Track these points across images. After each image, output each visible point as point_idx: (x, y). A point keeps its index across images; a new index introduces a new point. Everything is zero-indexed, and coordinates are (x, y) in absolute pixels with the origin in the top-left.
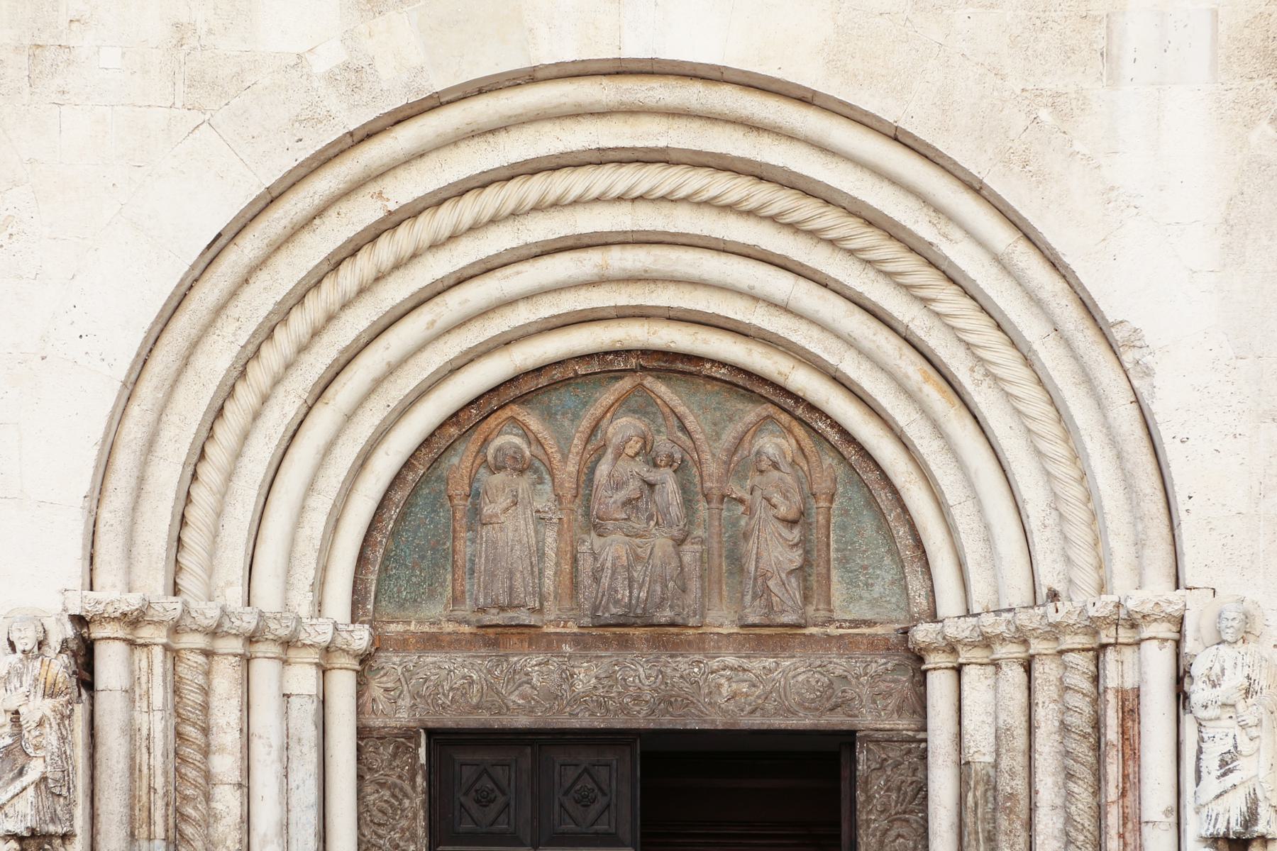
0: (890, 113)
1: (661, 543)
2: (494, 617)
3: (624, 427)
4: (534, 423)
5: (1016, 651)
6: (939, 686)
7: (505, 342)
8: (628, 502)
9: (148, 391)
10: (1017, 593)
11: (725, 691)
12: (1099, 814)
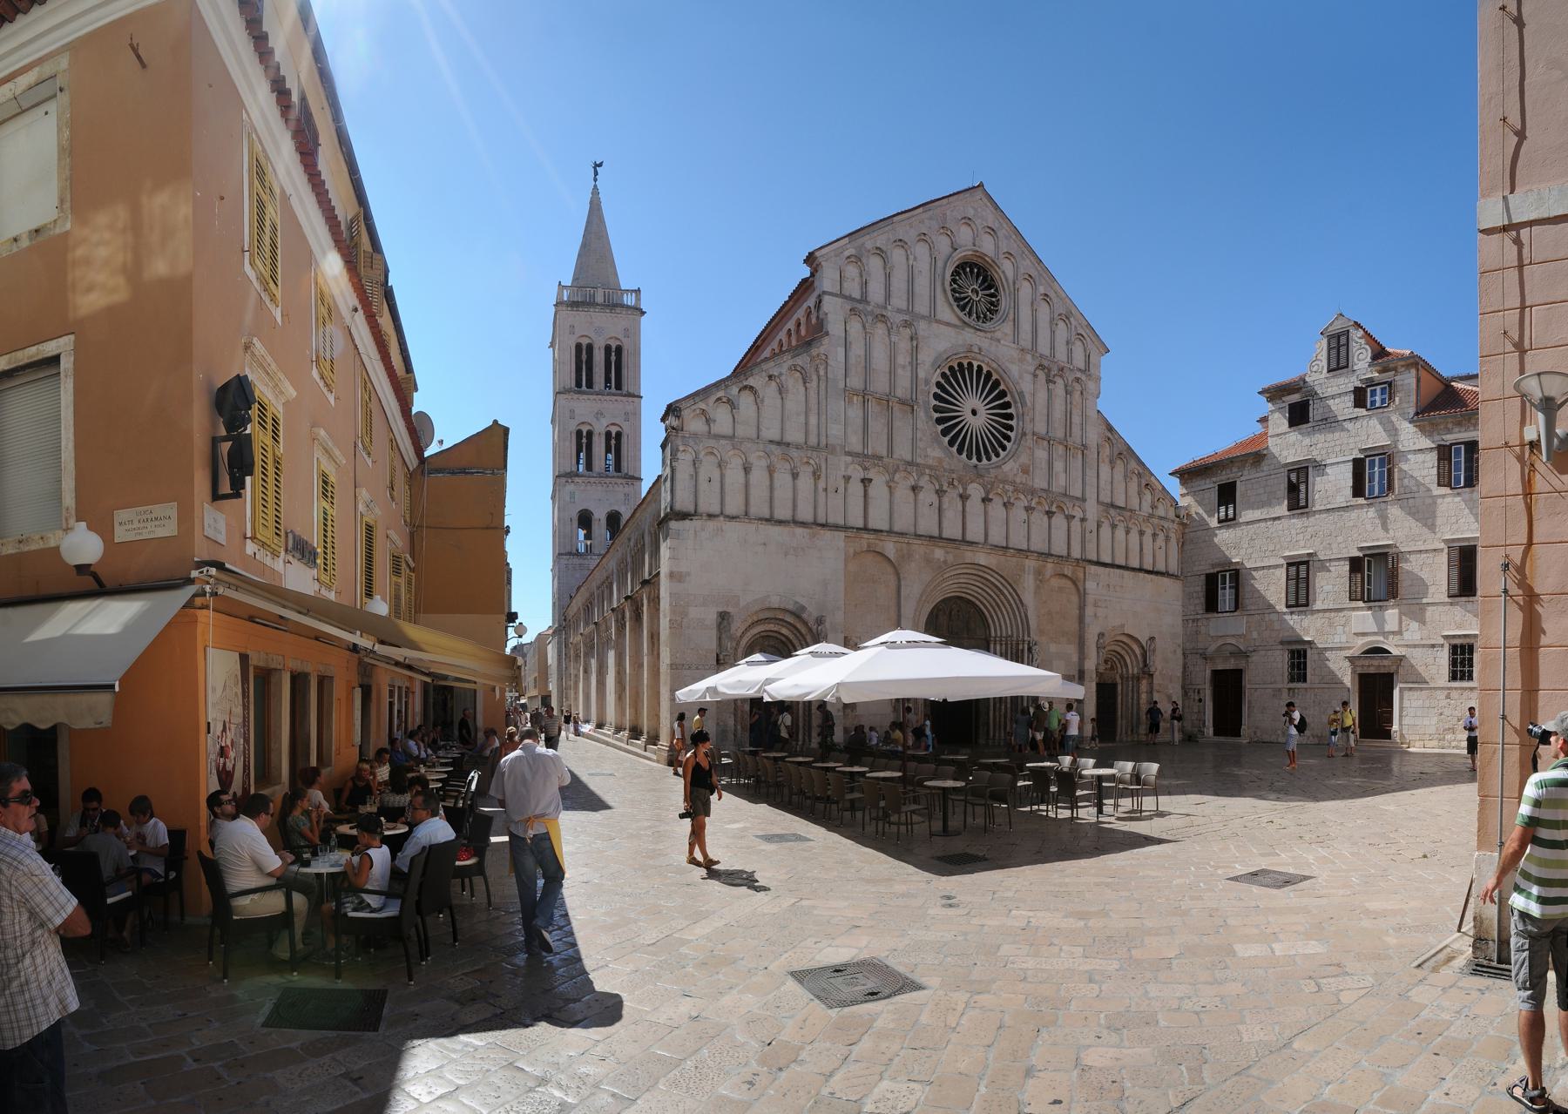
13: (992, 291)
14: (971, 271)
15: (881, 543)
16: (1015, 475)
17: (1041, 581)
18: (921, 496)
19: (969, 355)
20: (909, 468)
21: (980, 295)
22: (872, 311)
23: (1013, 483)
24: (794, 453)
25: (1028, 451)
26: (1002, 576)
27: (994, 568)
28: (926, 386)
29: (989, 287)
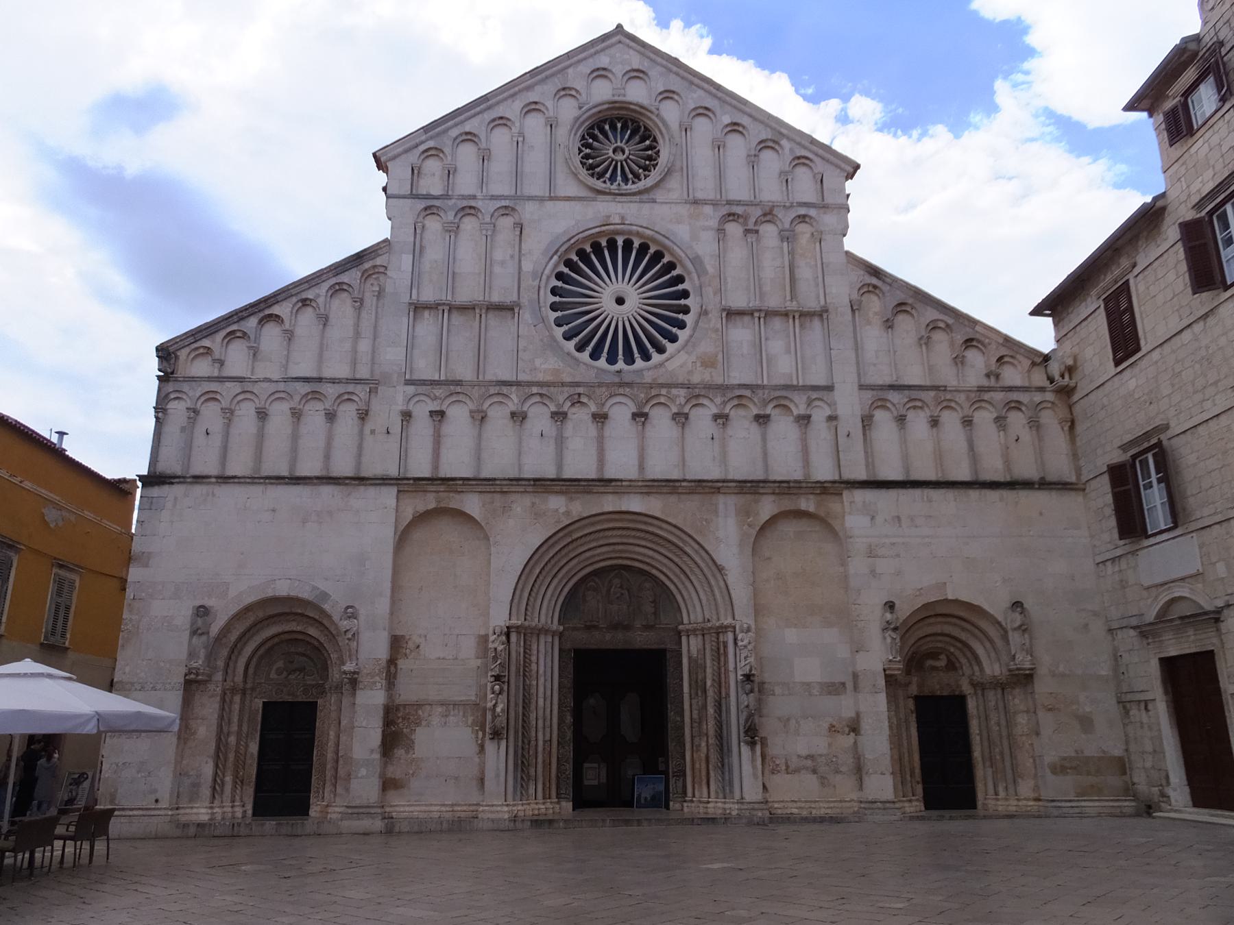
0: (674, 522)
1: (625, 607)
2: (588, 624)
3: (617, 581)
4: (597, 580)
5: (701, 632)
6: (684, 639)
7: (592, 564)
8: (618, 598)
9: (523, 578)
10: (700, 619)
11: (639, 639)
12: (719, 669)
13: (648, 142)
14: (613, 127)
15: (457, 496)
16: (690, 372)
17: (750, 526)
18: (528, 424)
19: (604, 228)
20: (505, 390)
21: (627, 152)
22: (455, 204)
23: (687, 386)
24: (331, 391)
25: (713, 336)
26: (675, 526)
27: (658, 514)
28: (533, 281)
29: (643, 140)
